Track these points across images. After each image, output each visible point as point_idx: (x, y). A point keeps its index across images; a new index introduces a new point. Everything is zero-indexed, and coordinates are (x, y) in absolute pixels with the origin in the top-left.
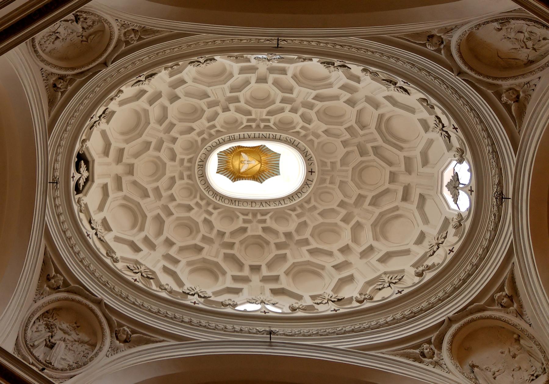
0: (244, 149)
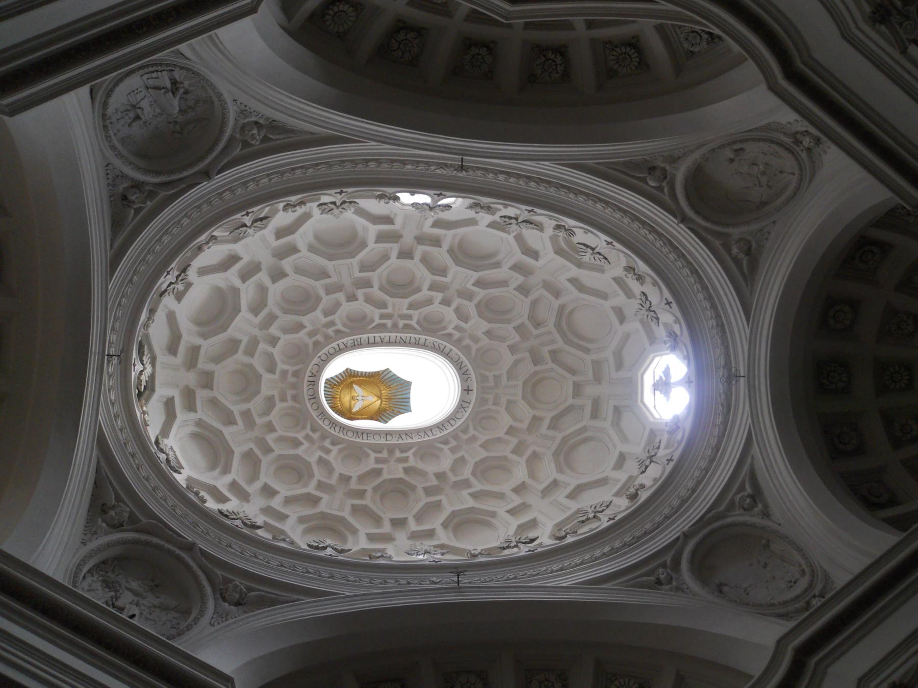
0: (358, 378)
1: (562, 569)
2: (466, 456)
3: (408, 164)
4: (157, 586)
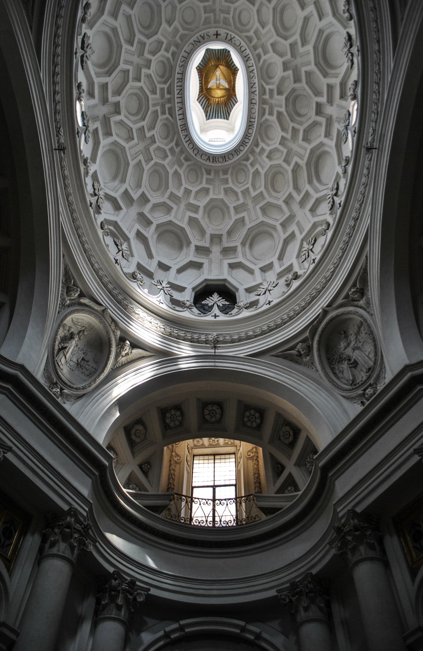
1: (378, 42)
2: (271, 41)
3: (65, 175)
4: (345, 333)
